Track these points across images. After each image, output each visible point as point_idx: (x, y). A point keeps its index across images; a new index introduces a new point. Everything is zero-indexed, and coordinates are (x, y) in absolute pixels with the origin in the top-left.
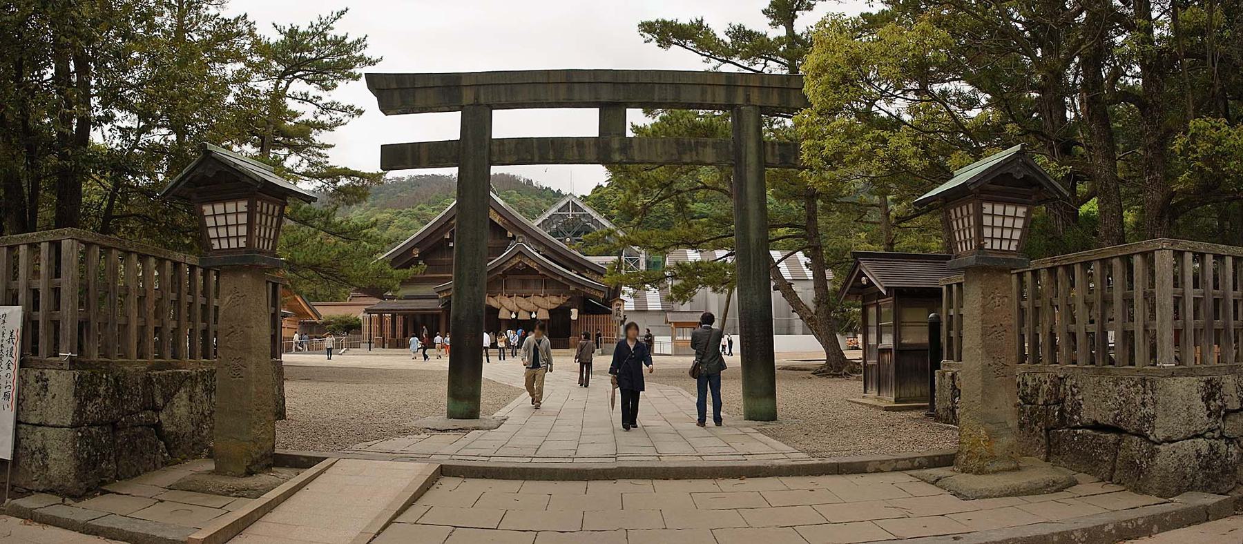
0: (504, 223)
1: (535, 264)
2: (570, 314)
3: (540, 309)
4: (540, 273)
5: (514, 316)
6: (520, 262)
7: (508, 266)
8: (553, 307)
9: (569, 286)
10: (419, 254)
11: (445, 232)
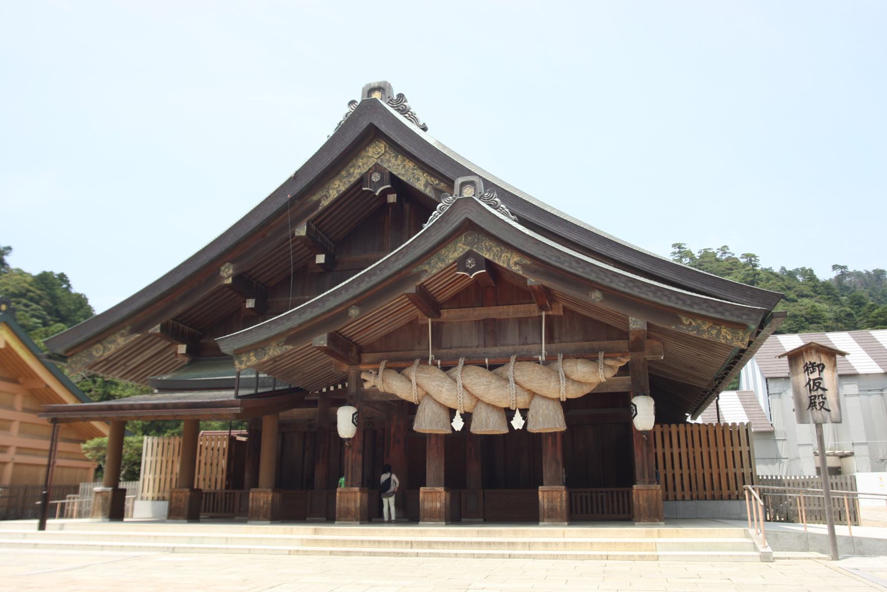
1: (516, 258)
2: (629, 412)
3: (537, 401)
4: (532, 281)
5: (458, 424)
6: (469, 254)
8: (574, 392)
11: (296, 222)
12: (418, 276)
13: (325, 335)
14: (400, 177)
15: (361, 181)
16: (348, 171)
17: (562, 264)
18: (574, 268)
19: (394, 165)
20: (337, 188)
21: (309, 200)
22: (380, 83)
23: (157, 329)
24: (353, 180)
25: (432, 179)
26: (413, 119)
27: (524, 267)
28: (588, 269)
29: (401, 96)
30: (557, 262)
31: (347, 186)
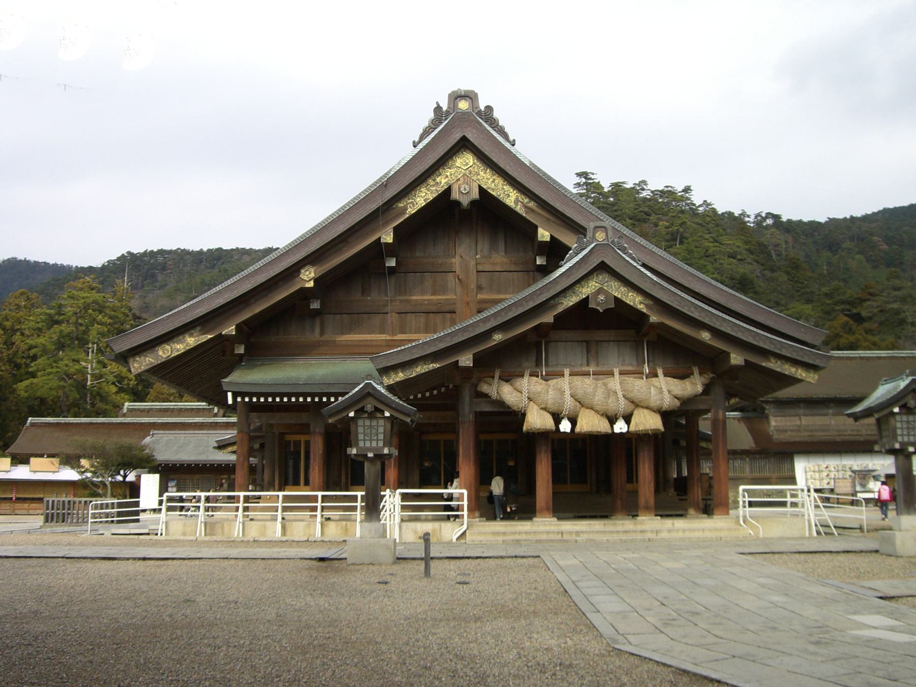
0: (526, 207)
4: (654, 319)
6: (600, 291)
7: (570, 301)
9: (727, 355)
10: (316, 280)
12: (555, 306)
13: (471, 356)
14: (489, 190)
15: (448, 191)
16: (434, 180)
17: (682, 307)
18: (692, 313)
19: (483, 178)
20: (422, 198)
21: (394, 206)
22: (465, 91)
23: (230, 330)
24: (441, 190)
25: (523, 197)
26: (505, 136)
27: (647, 306)
28: (703, 314)
29: (489, 108)
30: (679, 306)
31: (435, 196)
